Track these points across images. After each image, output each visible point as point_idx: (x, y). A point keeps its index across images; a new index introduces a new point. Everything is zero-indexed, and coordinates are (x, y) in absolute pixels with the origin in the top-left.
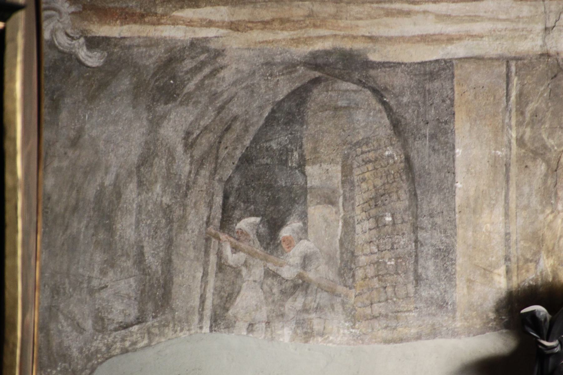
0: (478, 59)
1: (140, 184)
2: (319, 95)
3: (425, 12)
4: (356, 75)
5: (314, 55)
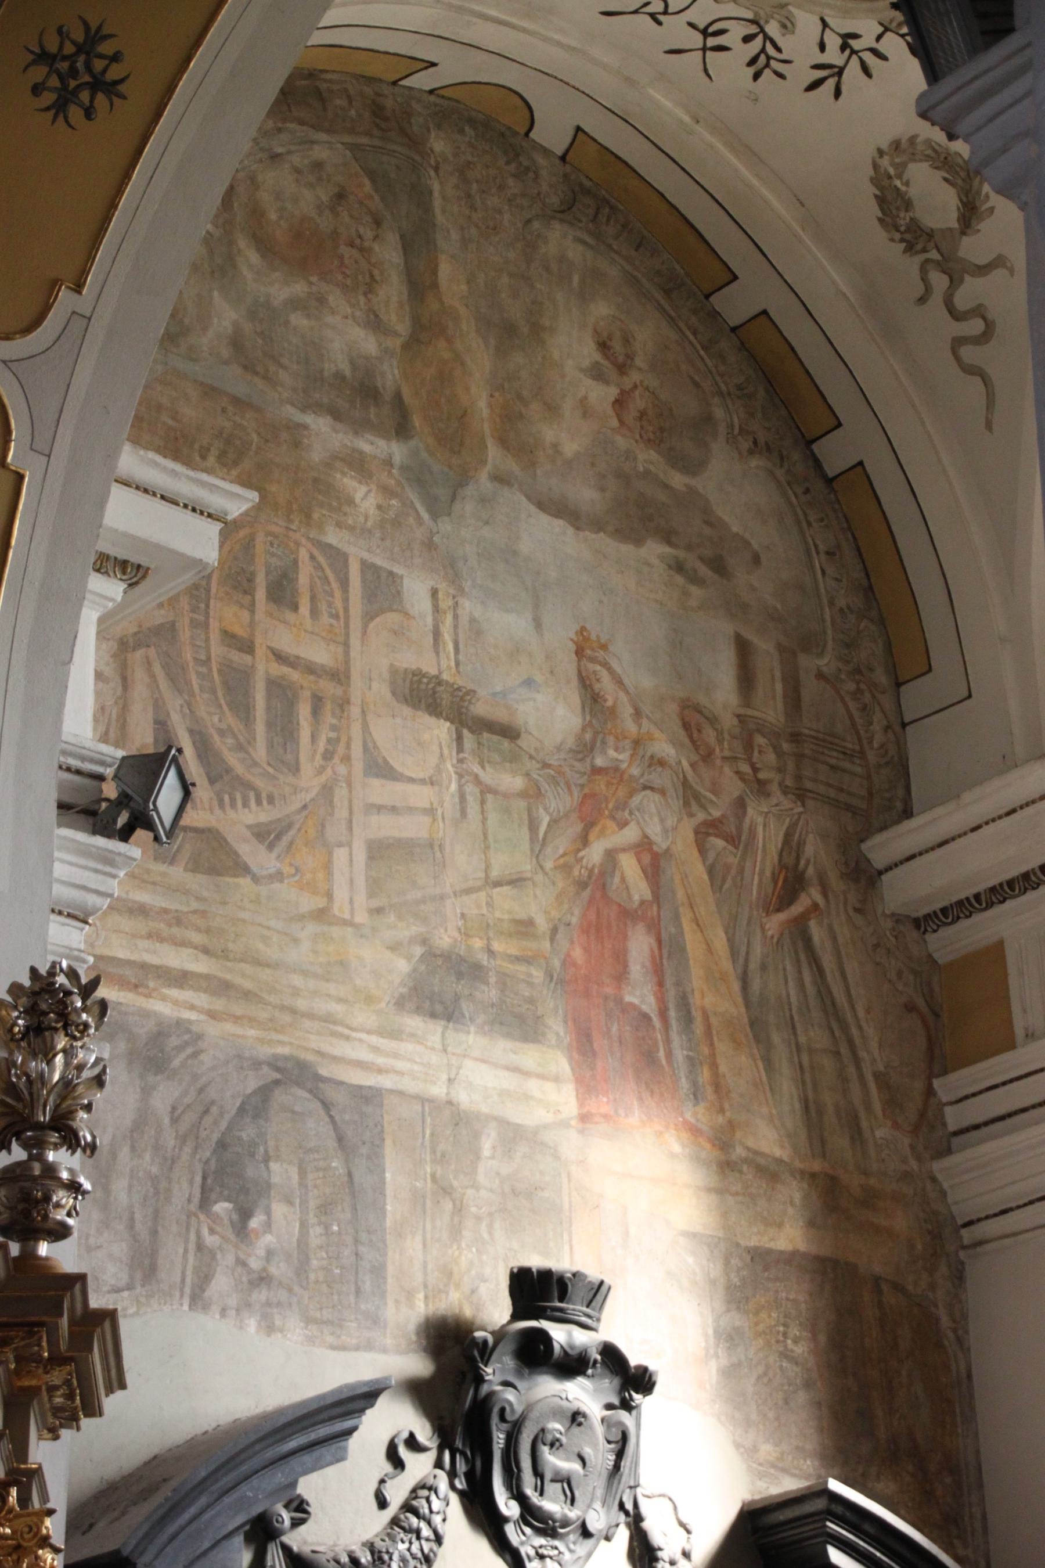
0: (401, 1093)
1: (133, 1148)
2: (279, 1096)
3: (361, 1040)
4: (309, 1085)
5: (276, 1057)
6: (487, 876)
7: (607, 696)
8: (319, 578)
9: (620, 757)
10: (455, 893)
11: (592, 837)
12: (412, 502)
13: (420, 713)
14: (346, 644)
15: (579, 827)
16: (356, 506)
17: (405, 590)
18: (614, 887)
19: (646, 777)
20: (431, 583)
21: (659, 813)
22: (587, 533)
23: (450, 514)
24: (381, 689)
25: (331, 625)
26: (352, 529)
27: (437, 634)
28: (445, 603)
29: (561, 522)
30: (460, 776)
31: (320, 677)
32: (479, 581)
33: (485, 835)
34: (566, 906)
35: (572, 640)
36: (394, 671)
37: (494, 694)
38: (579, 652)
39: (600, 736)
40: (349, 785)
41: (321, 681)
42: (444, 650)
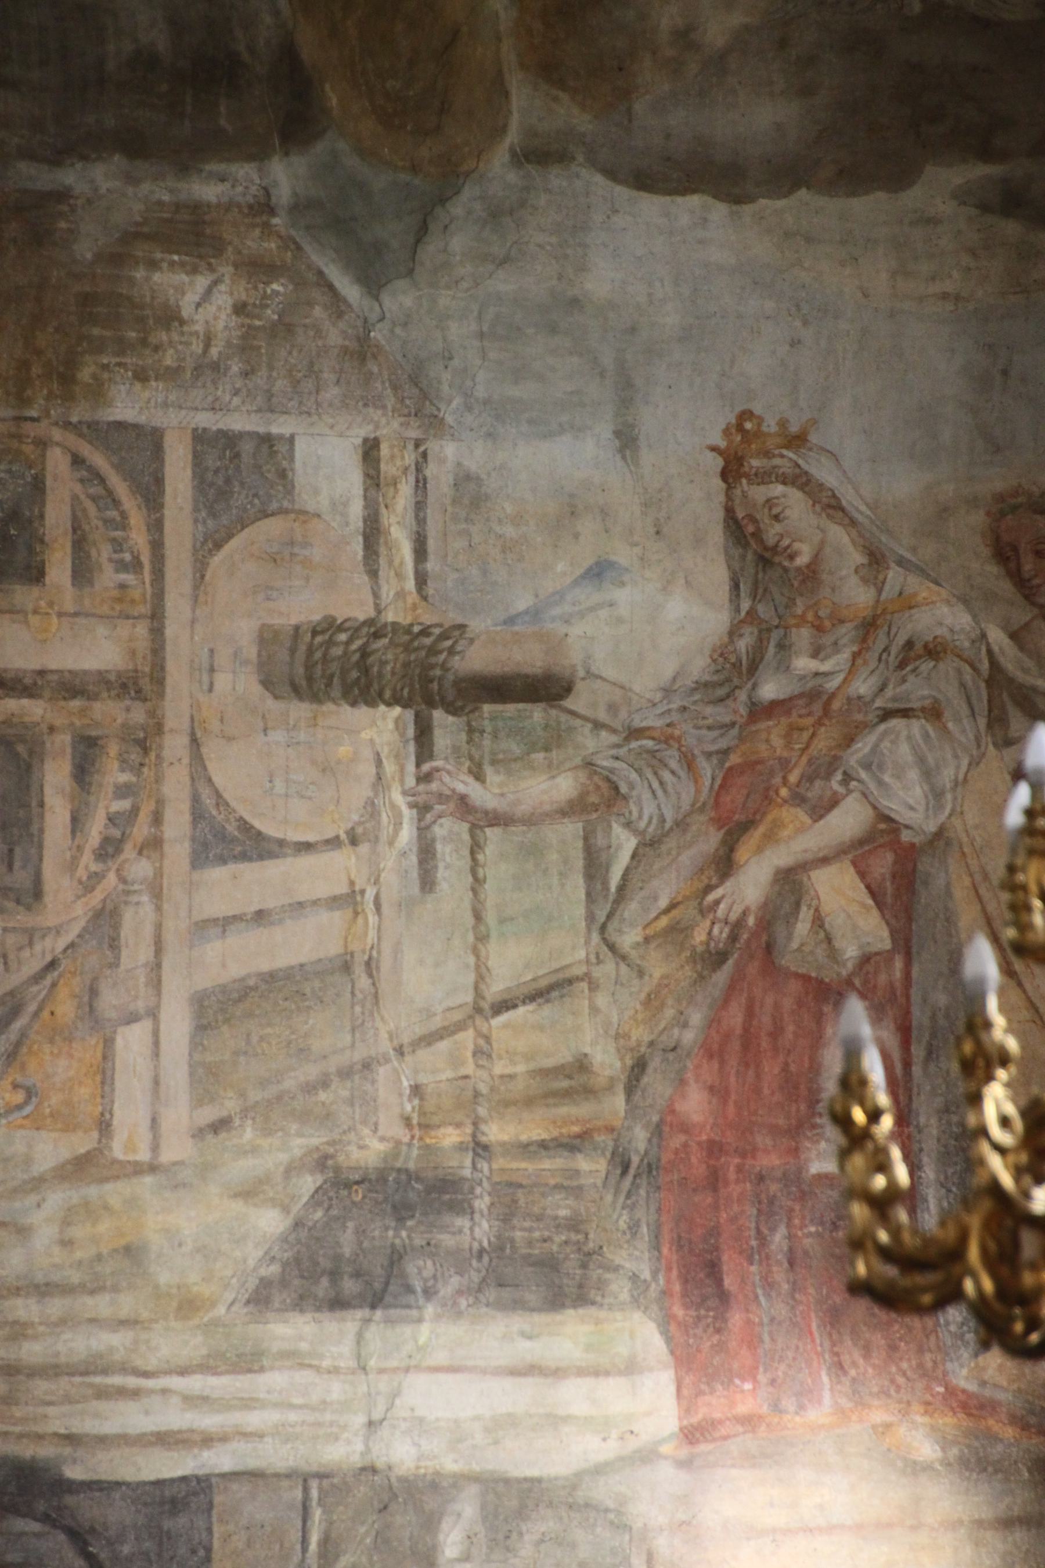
6: (478, 994)
7: (797, 546)
8: (94, 499)
9: (825, 667)
10: (400, 1051)
11: (742, 854)
12: (320, 273)
13: (329, 706)
14: (157, 617)
15: (711, 841)
16: (182, 322)
17: (298, 464)
18: (794, 945)
19: (889, 692)
20: (361, 432)
21: (921, 760)
22: (763, 202)
23: (410, 272)
24: (238, 683)
25: (123, 586)
26: (172, 375)
27: (373, 534)
28: (395, 461)
29: (695, 200)
30: (422, 809)
31: (93, 697)
32: (480, 392)
33: (478, 916)
34: (669, 1013)
35: (714, 449)
36: (267, 637)
37: (510, 621)
38: (732, 469)
39: (776, 636)
40: (157, 894)
41: (97, 706)
42: (390, 562)
